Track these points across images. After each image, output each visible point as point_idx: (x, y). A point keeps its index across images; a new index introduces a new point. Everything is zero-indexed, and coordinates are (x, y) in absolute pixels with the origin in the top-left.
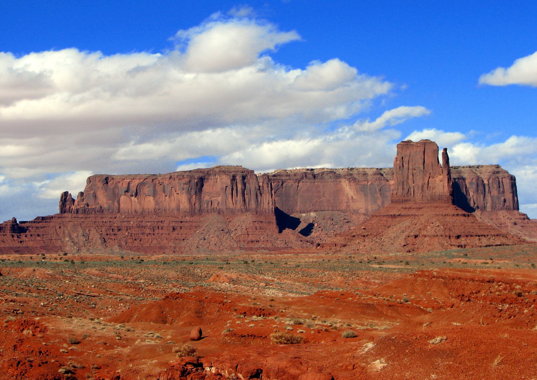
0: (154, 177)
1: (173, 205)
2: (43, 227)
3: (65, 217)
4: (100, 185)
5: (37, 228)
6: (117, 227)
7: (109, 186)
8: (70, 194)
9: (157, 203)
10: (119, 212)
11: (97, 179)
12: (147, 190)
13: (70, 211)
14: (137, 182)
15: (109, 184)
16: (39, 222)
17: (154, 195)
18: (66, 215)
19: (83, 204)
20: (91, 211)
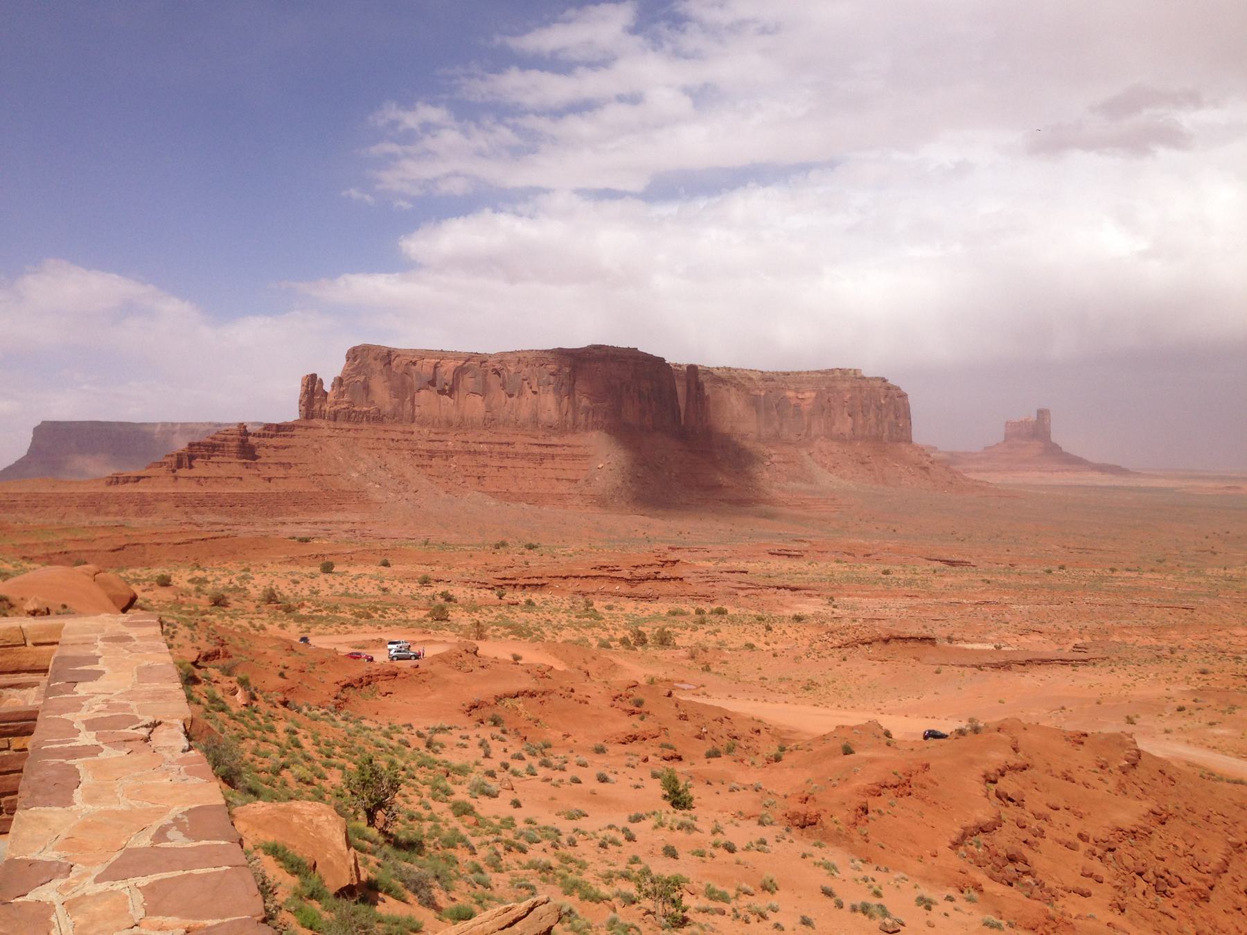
0: (482, 359)
1: (525, 413)
2: (285, 448)
3: (318, 428)
4: (378, 366)
5: (275, 447)
6: (427, 451)
7: (394, 369)
8: (321, 380)
9: (489, 409)
10: (413, 422)
11: (372, 355)
12: (468, 381)
13: (322, 416)
14: (449, 366)
15: (394, 364)
16: (272, 436)
17: (484, 391)
18: (315, 422)
19: (347, 402)
20: (361, 416)
